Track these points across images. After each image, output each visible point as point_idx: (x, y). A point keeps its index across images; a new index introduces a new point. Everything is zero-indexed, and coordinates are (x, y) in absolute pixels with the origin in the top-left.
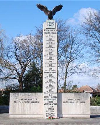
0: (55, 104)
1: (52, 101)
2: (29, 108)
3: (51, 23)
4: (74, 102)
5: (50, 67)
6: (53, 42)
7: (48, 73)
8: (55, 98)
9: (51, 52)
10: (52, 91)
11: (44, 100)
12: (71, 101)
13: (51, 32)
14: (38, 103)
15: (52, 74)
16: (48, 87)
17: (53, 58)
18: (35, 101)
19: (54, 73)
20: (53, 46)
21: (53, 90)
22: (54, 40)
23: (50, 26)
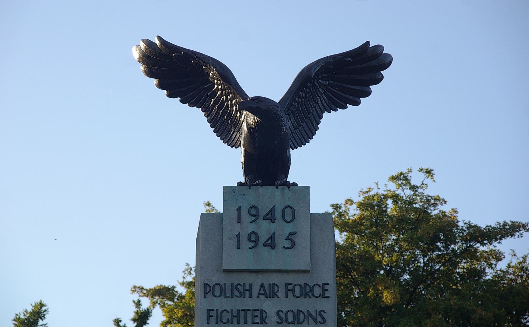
3: (270, 217)
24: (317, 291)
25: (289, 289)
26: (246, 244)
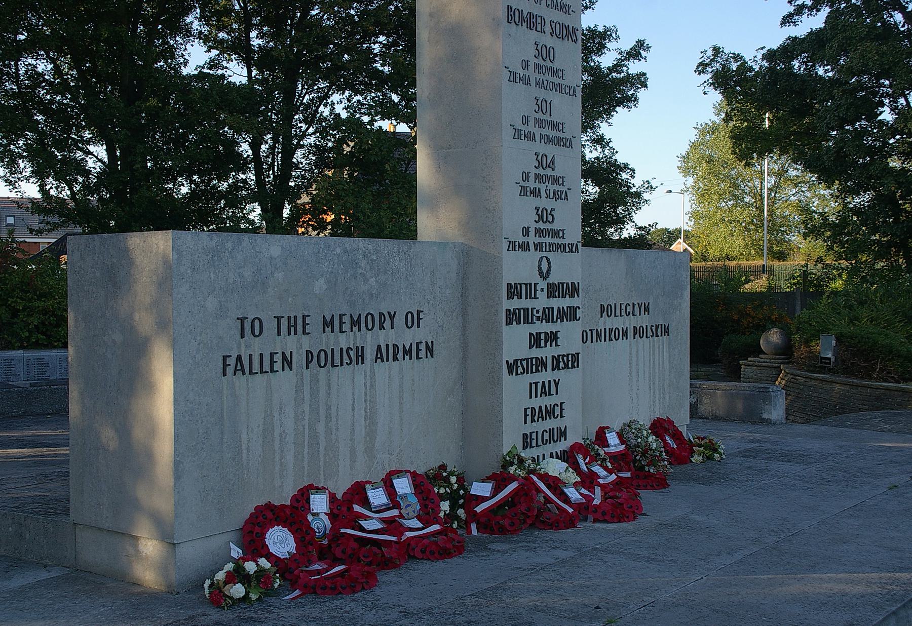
4: (328, 324)
11: (512, 317)
14: (427, 363)
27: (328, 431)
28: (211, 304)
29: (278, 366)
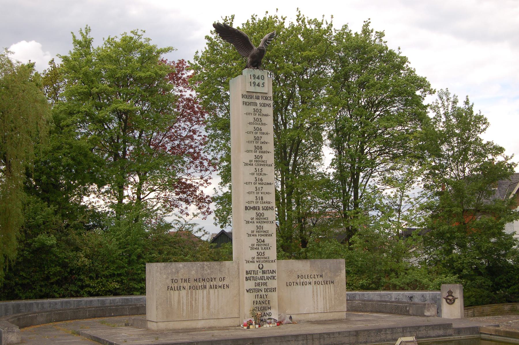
0: (274, 290)
1: (265, 282)
2: (205, 303)
3: (258, 78)
5: (258, 193)
6: (263, 127)
7: (254, 208)
8: (271, 275)
9: (260, 154)
10: (265, 256)
11: (247, 279)
12: (305, 280)
13: (258, 102)
14: (227, 290)
15: (265, 212)
16: (255, 246)
17: (266, 170)
18: (221, 284)
19: (267, 209)
20: (265, 138)
21: (267, 253)
22: (265, 124)
23: (257, 87)
24: (269, 98)
25: (262, 98)
26: (252, 85)
27: (196, 303)
28: (165, 276)
29: (182, 289)
